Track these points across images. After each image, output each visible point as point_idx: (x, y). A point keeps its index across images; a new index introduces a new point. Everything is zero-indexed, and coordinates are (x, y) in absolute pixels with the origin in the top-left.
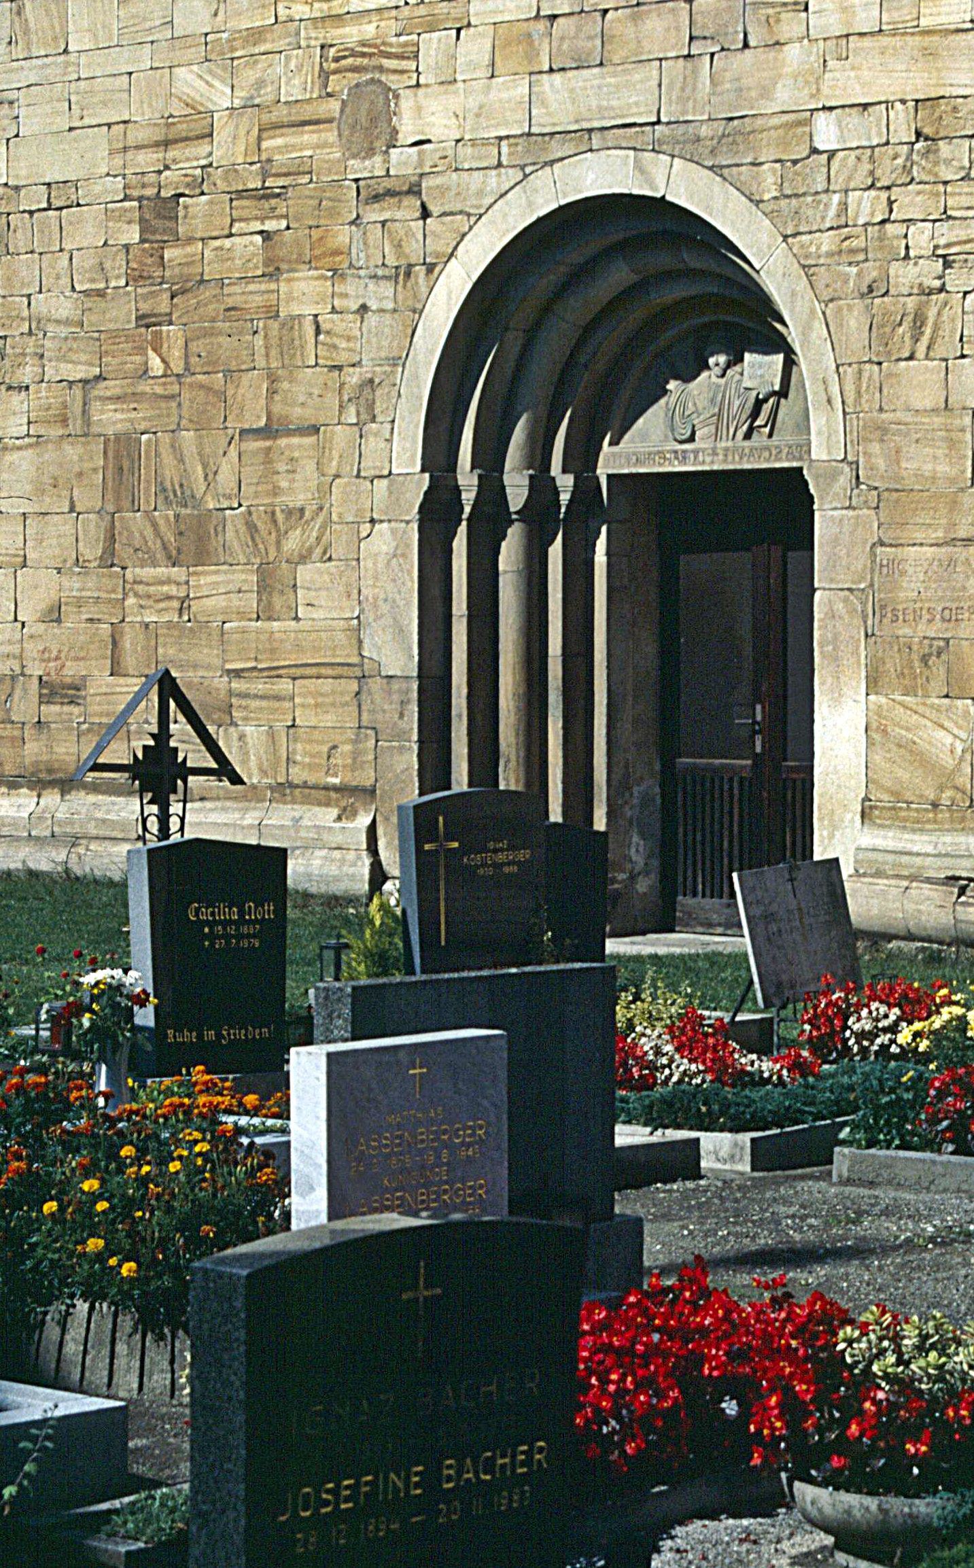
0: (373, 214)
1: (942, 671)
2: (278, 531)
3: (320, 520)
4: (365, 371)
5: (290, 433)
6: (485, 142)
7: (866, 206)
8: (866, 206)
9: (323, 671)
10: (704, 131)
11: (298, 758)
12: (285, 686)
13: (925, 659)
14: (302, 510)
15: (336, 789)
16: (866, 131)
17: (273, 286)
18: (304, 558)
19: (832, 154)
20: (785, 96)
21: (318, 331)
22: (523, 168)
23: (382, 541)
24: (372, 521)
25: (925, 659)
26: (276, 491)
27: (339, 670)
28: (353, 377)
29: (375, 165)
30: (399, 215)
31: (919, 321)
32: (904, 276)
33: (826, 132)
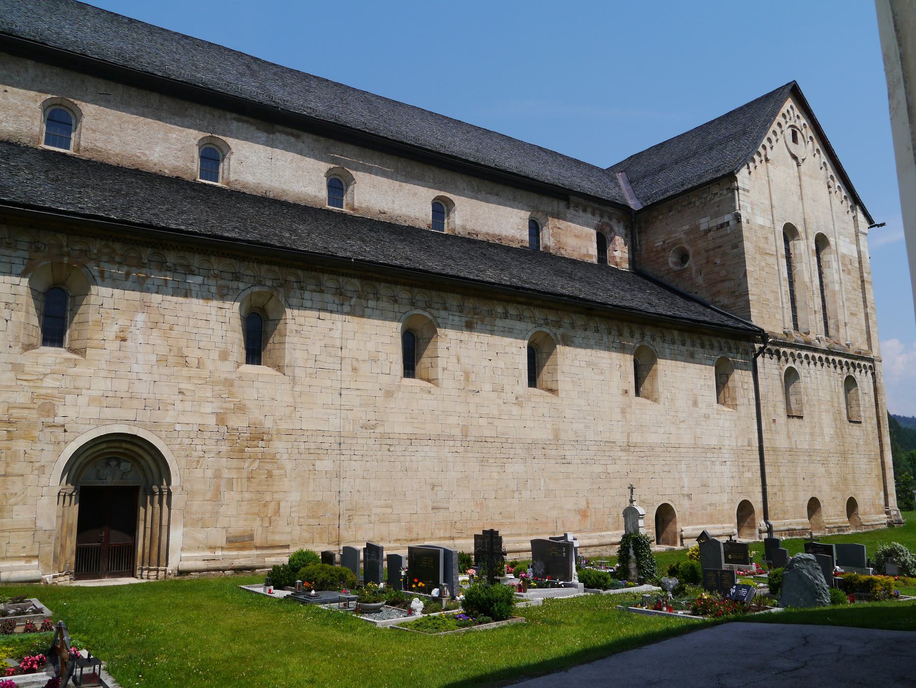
0: (49, 430)
1: (201, 524)
2: (7, 498)
3: (23, 495)
4: (42, 464)
5: (13, 476)
6: (86, 419)
7: (187, 441)
8: (187, 441)
9: (22, 530)
10: (148, 423)
11: (10, 550)
12: (6, 534)
13: (197, 521)
14: (16, 494)
15: (24, 557)
16: (189, 428)
17: (10, 443)
18: (16, 504)
19: (179, 431)
20: (168, 420)
21: (26, 453)
22: (97, 425)
23: (45, 500)
24: (42, 496)
25: (197, 521)
26: (7, 489)
27: (26, 530)
28: (37, 465)
29: (50, 420)
30: (56, 431)
31: (198, 462)
32: (195, 454)
33: (178, 427)
